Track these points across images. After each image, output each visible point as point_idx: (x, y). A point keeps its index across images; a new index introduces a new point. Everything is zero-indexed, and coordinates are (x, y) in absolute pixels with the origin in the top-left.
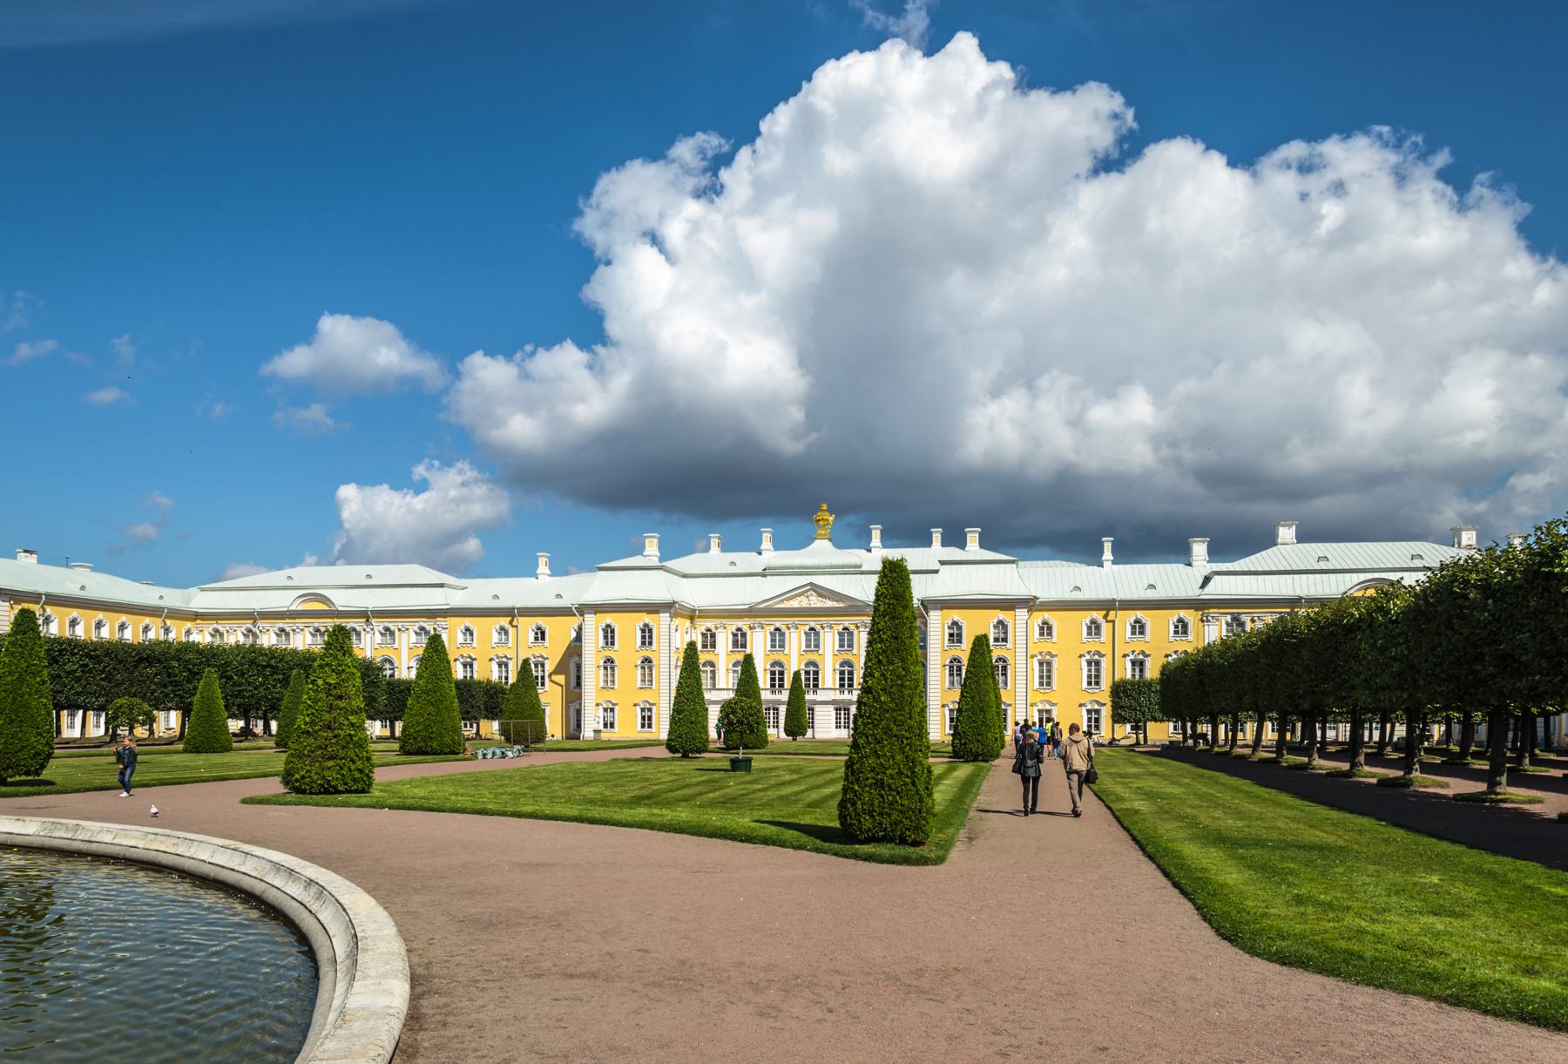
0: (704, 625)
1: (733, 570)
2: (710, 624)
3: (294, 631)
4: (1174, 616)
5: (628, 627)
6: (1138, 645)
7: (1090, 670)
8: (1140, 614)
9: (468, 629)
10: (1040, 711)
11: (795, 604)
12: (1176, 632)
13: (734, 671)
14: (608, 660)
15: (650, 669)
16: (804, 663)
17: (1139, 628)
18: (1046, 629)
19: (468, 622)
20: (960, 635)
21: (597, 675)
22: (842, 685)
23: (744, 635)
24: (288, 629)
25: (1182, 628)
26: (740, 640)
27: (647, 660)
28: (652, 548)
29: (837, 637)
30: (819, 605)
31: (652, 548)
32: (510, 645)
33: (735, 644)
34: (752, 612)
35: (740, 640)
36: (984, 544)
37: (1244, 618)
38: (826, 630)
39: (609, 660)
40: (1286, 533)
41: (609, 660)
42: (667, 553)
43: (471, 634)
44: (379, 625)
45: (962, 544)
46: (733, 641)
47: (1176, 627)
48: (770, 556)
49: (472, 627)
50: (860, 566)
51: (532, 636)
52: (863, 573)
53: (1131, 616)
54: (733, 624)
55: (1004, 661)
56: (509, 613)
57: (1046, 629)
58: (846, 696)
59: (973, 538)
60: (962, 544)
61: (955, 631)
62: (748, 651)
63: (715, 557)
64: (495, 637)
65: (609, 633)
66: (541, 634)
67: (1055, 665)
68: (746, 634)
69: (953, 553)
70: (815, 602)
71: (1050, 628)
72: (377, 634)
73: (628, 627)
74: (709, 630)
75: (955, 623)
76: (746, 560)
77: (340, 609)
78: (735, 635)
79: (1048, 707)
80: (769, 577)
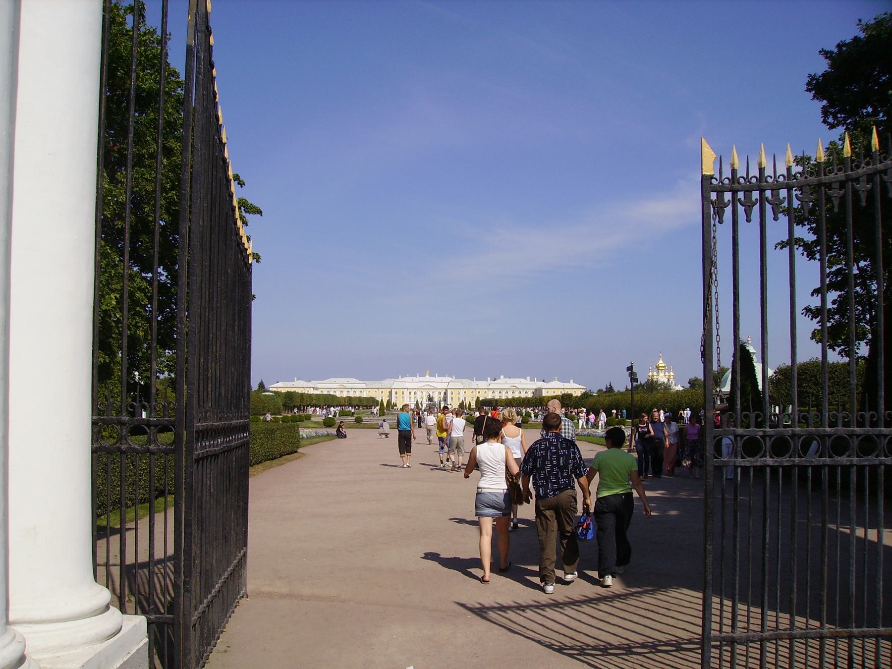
0: (409, 390)
6: (478, 395)
11: (425, 387)
17: (479, 392)
19: (369, 390)
25: (486, 392)
26: (415, 393)
28: (400, 377)
31: (400, 377)
35: (415, 393)
40: (502, 377)
44: (353, 390)
59: (454, 377)
65: (396, 393)
66: (382, 392)
69: (449, 379)
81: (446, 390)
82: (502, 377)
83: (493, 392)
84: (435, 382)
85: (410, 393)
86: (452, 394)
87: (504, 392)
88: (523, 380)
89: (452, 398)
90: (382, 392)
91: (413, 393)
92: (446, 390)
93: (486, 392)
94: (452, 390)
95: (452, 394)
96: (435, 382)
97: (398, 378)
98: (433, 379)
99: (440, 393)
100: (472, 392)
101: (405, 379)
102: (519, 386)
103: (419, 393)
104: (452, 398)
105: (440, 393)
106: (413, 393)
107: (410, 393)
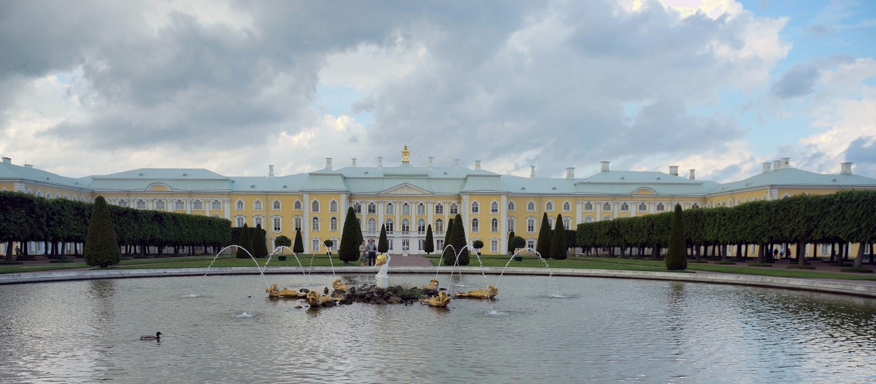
3: (147, 201)
7: (529, 224)
9: (240, 202)
10: (529, 242)
11: (398, 192)
12: (565, 209)
13: (369, 223)
14: (316, 218)
15: (336, 222)
16: (418, 219)
20: (477, 208)
21: (310, 223)
22: (419, 230)
23: (374, 206)
24: (125, 200)
25: (567, 207)
26: (372, 210)
29: (417, 207)
30: (410, 193)
32: (262, 210)
33: (370, 211)
34: (378, 196)
35: (372, 210)
37: (591, 203)
38: (412, 204)
43: (242, 204)
46: (369, 210)
47: (565, 206)
49: (242, 201)
50: (427, 176)
51: (273, 206)
52: (429, 179)
55: (496, 220)
58: (421, 235)
61: (475, 206)
62: (458, 213)
64: (254, 206)
67: (515, 222)
68: (375, 206)
71: (513, 206)
72: (193, 203)
74: (357, 204)
75: (475, 203)
77: (174, 191)
78: (370, 206)
79: (532, 240)
80: (385, 180)
81: (459, 197)
83: (589, 206)
86: (475, 210)
89: (475, 223)
90: (277, 206)
92: (459, 197)
93: (567, 207)
95: (475, 210)
99: (439, 209)
100: (531, 206)
103: (381, 209)
104: (475, 223)
105: (439, 209)
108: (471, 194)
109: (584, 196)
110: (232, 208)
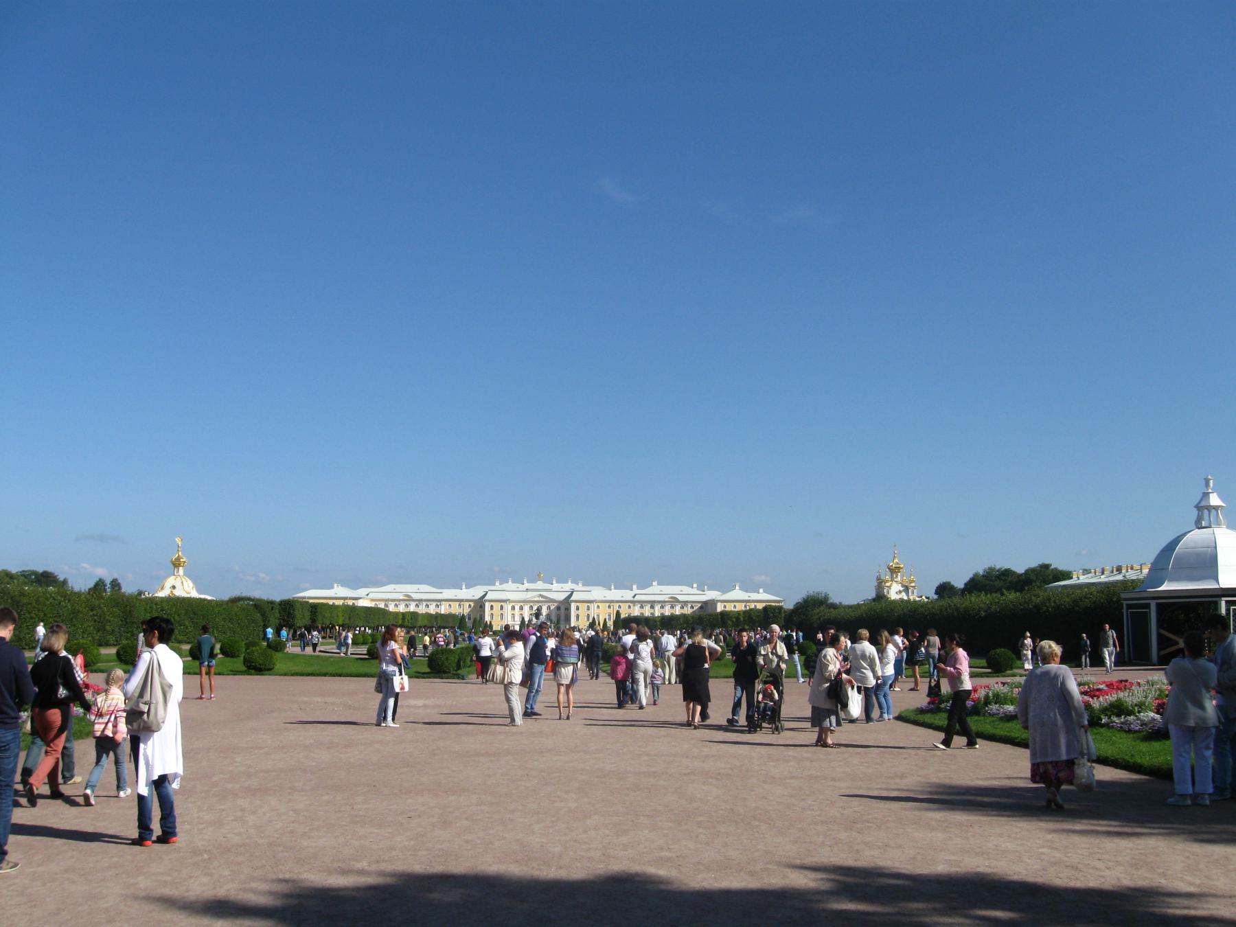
1: (517, 589)
2: (514, 604)
4: (627, 605)
5: (497, 606)
8: (620, 604)
18: (598, 607)
25: (629, 607)
26: (521, 608)
27: (502, 614)
31: (497, 584)
34: (525, 602)
35: (521, 608)
36: (583, 585)
39: (492, 614)
40: (655, 583)
41: (492, 614)
42: (500, 584)
44: (425, 603)
45: (578, 585)
48: (527, 585)
53: (618, 604)
54: (519, 604)
56: (462, 601)
57: (598, 607)
59: (580, 585)
60: (578, 585)
63: (510, 585)
65: (492, 607)
70: (541, 599)
73: (497, 606)
76: (522, 587)
82: (655, 583)
84: (550, 590)
85: (513, 608)
87: (657, 608)
88: (686, 589)
89: (578, 617)
91: (517, 608)
93: (629, 607)
94: (578, 604)
96: (550, 590)
97: (494, 585)
98: (547, 586)
101: (504, 586)
102: (681, 598)
103: (526, 608)
104: (578, 617)
106: (517, 608)
107: (513, 608)
108: (576, 601)
109: (639, 602)
110: (445, 607)
